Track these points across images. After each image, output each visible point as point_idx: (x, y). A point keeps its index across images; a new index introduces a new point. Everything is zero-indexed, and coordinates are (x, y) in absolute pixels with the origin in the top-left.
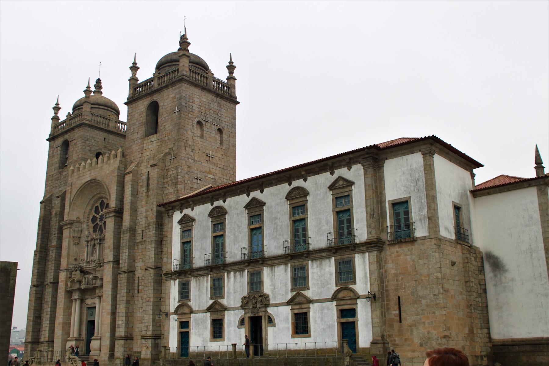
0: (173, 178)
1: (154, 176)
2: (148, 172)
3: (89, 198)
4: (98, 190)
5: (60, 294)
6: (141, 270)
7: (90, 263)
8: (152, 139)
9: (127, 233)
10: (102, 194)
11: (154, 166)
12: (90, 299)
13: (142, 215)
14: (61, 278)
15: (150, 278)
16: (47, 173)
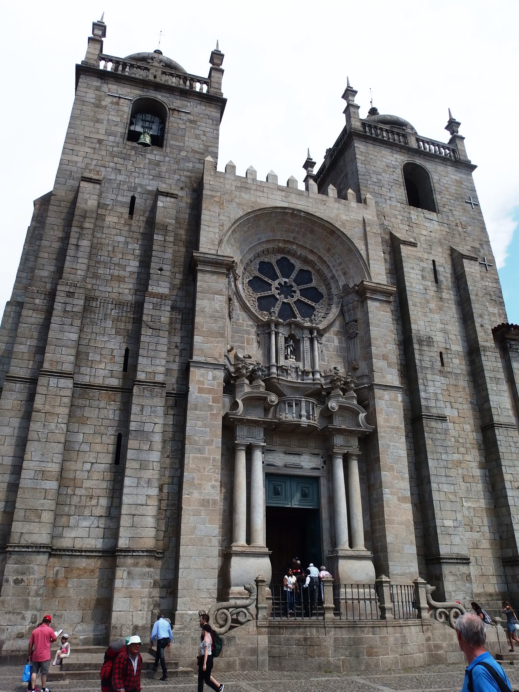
0: (492, 293)
1: (474, 274)
2: (434, 261)
3: (260, 239)
4: (292, 235)
5: (199, 423)
6: (452, 424)
7: (289, 372)
8: (428, 216)
9: (428, 345)
10: (294, 247)
11: (471, 259)
12: (283, 455)
13: (434, 324)
14: (203, 383)
15: (512, 444)
16: (71, 126)
